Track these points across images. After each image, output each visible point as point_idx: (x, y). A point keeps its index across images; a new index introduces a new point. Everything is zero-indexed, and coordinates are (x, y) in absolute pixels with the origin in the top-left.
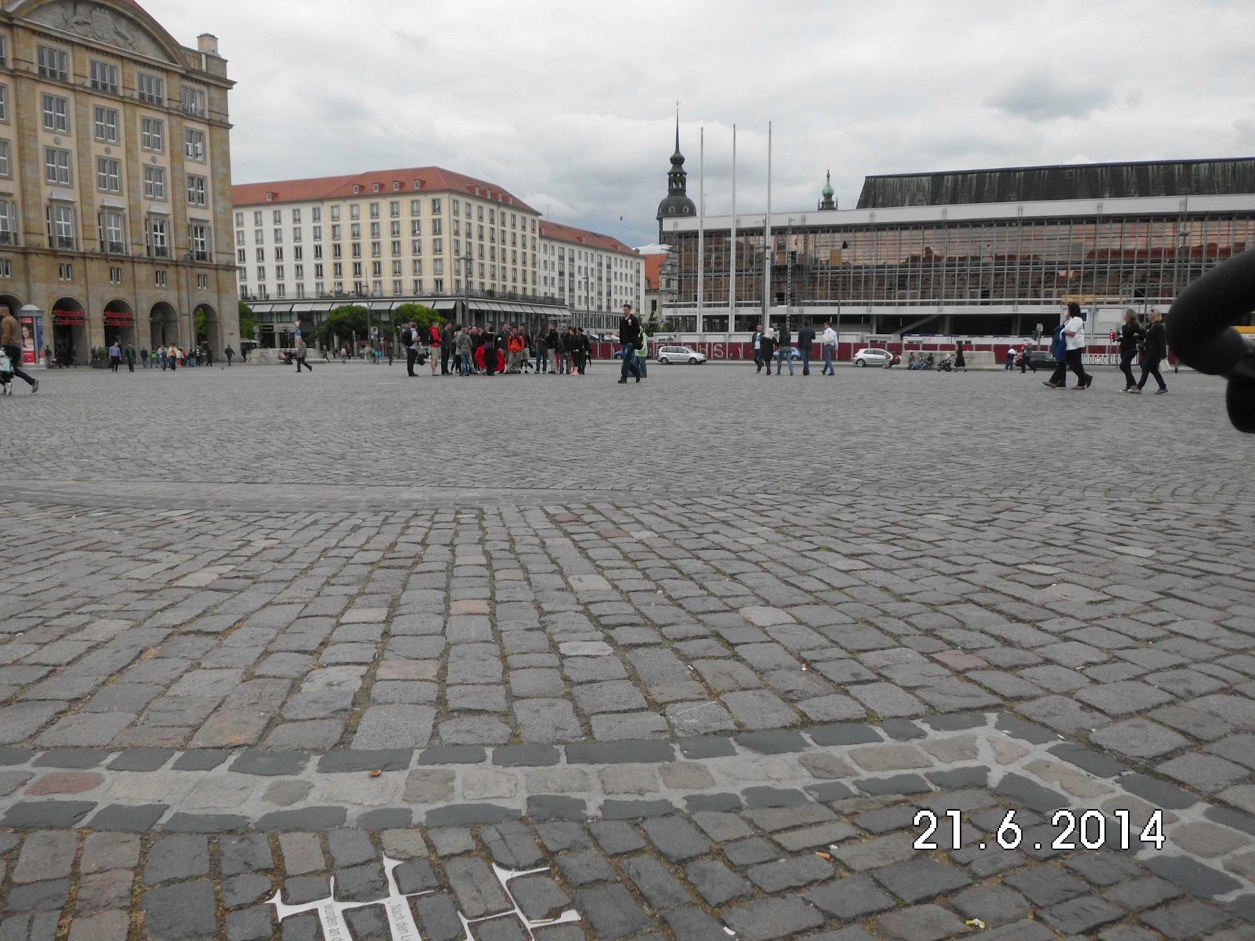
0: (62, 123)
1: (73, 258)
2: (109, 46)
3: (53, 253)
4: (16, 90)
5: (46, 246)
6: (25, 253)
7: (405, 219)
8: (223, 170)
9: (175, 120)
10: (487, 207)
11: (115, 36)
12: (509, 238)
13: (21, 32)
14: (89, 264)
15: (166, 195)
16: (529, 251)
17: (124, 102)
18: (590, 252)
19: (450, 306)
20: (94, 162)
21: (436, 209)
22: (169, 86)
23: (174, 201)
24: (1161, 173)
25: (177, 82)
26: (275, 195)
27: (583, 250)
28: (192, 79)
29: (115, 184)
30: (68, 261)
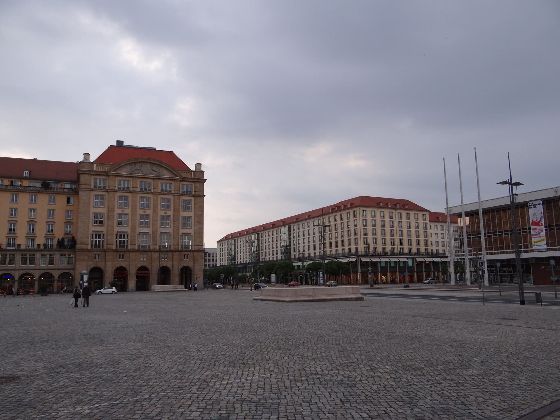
1: (124, 252)
3: (116, 251)
5: (114, 248)
6: (105, 251)
8: (200, 213)
9: (176, 197)
11: (151, 171)
13: (111, 177)
14: (131, 254)
16: (421, 230)
17: (153, 194)
19: (353, 260)
20: (138, 217)
22: (174, 185)
23: (174, 227)
25: (178, 183)
29: (147, 223)
30: (124, 253)
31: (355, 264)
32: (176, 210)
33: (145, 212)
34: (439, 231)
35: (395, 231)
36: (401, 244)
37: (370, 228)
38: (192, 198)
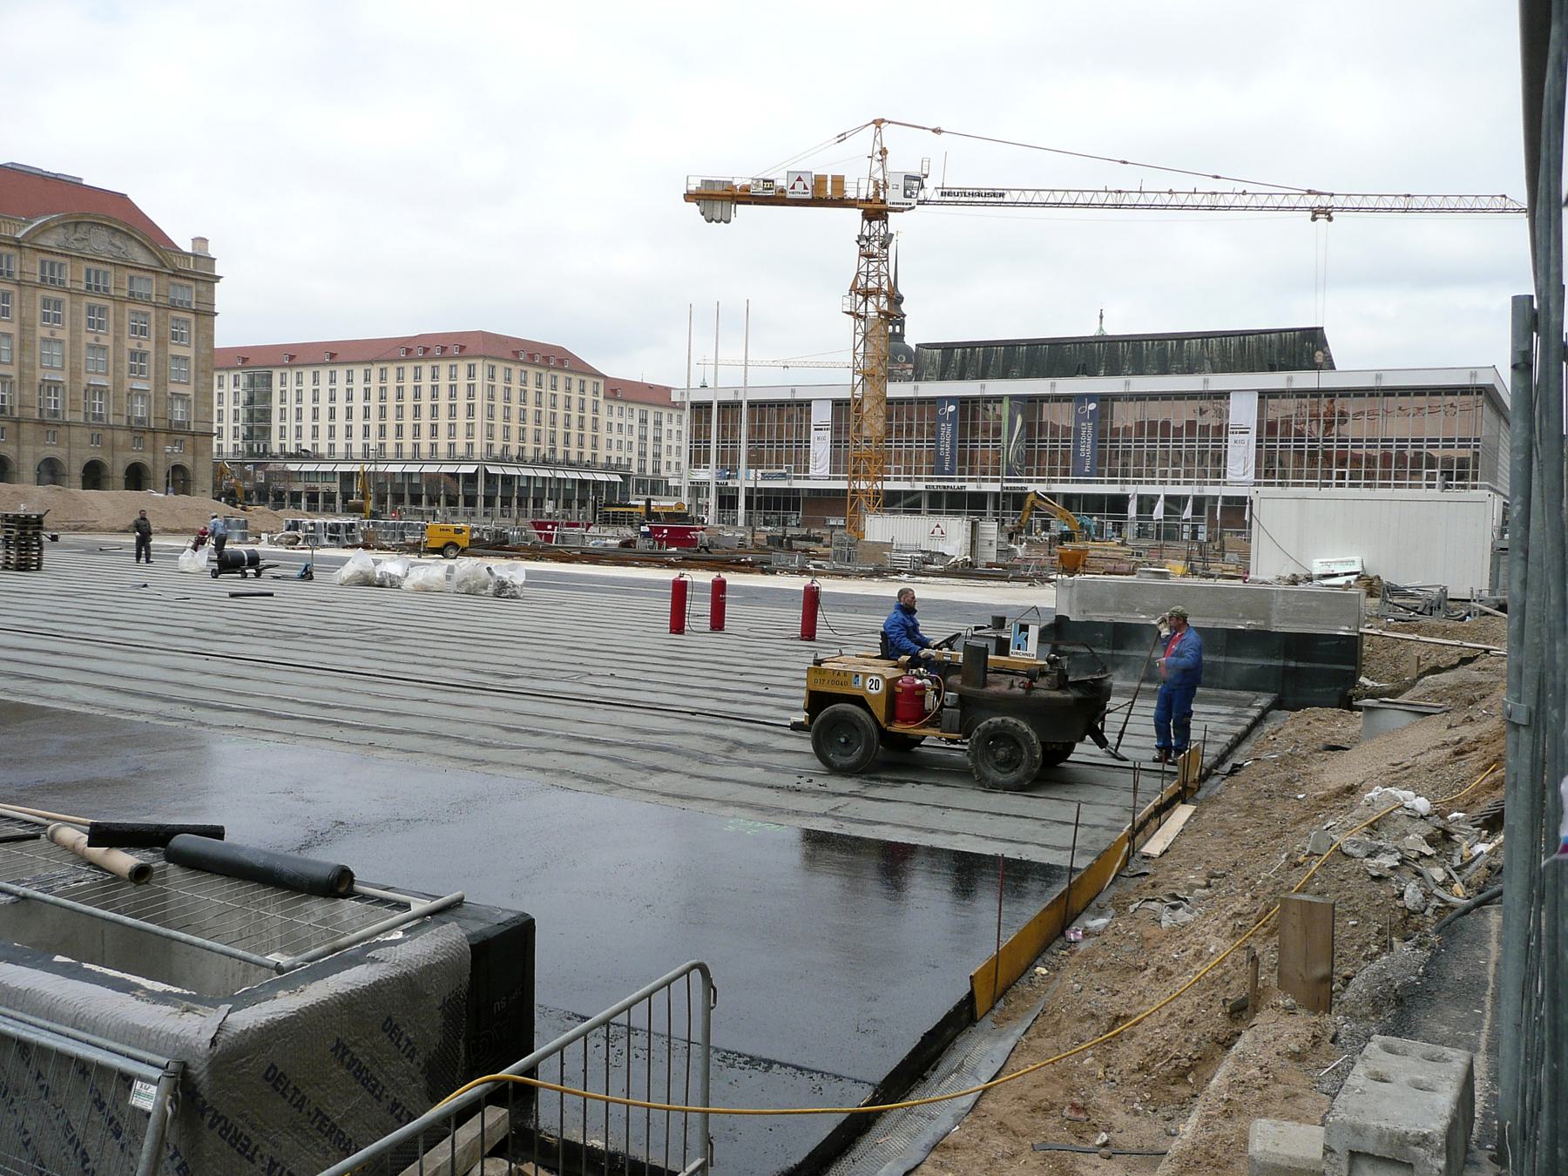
0: (57, 319)
2: (105, 256)
3: (42, 422)
4: (20, 295)
6: (18, 421)
7: (444, 383)
9: (161, 312)
10: (532, 372)
11: (109, 247)
12: (561, 402)
13: (27, 251)
14: (73, 430)
15: (149, 374)
16: (589, 415)
19: (471, 469)
23: (156, 378)
24: (1156, 348)
25: (164, 281)
26: (332, 355)
28: (176, 276)
31: (471, 479)
32: (160, 342)
33: (97, 339)
34: (616, 420)
35: (543, 414)
37: (499, 404)
38: (191, 317)
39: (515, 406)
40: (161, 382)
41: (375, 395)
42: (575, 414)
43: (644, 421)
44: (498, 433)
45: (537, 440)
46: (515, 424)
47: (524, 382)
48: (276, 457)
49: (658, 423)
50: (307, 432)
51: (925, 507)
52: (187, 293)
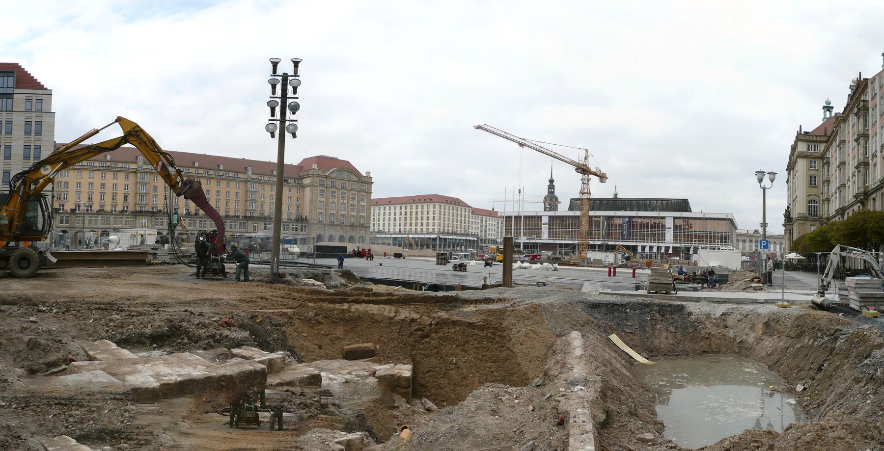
0: (334, 196)
2: (346, 179)
3: (330, 225)
6: (324, 225)
7: (425, 210)
10: (451, 206)
12: (459, 215)
16: (467, 219)
18: (494, 219)
19: (435, 236)
21: (434, 207)
25: (360, 184)
27: (491, 218)
31: (434, 239)
32: (358, 202)
36: (457, 228)
39: (447, 217)
40: (358, 213)
41: (403, 214)
42: (463, 219)
43: (482, 221)
44: (442, 225)
45: (453, 227)
46: (446, 222)
47: (449, 210)
48: (372, 233)
49: (486, 221)
50: (381, 225)
51: (597, 249)
52: (365, 187)
